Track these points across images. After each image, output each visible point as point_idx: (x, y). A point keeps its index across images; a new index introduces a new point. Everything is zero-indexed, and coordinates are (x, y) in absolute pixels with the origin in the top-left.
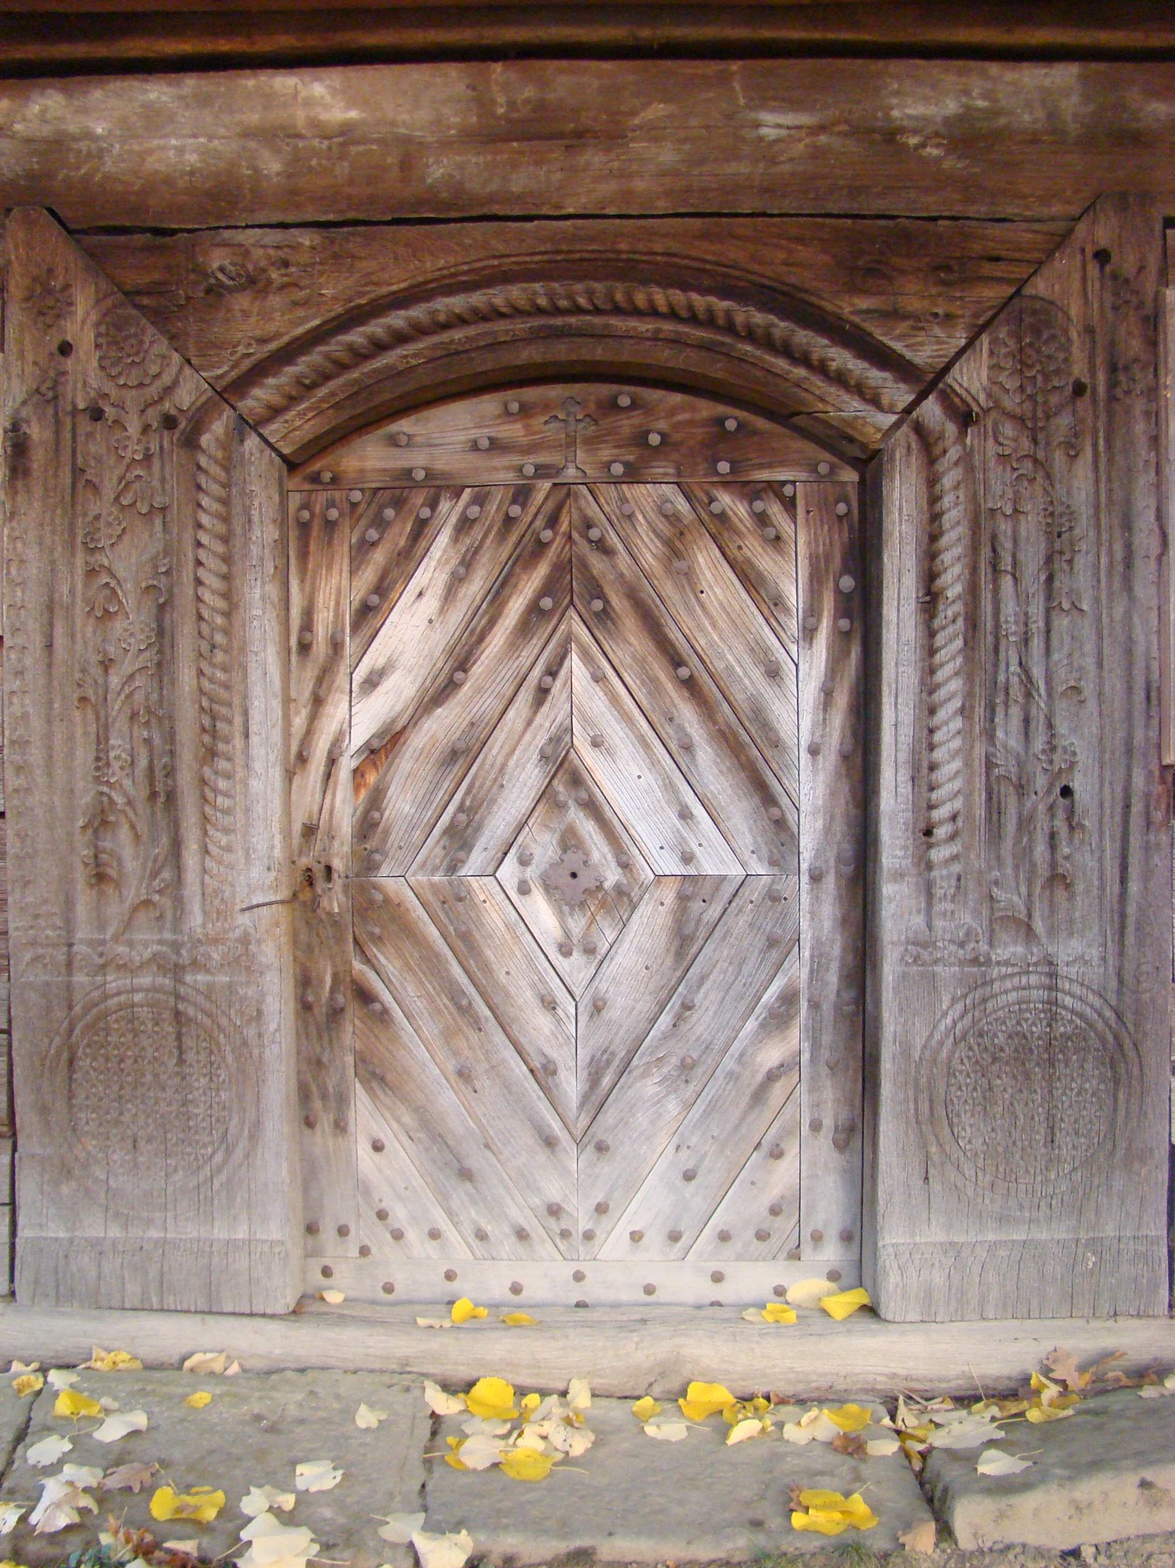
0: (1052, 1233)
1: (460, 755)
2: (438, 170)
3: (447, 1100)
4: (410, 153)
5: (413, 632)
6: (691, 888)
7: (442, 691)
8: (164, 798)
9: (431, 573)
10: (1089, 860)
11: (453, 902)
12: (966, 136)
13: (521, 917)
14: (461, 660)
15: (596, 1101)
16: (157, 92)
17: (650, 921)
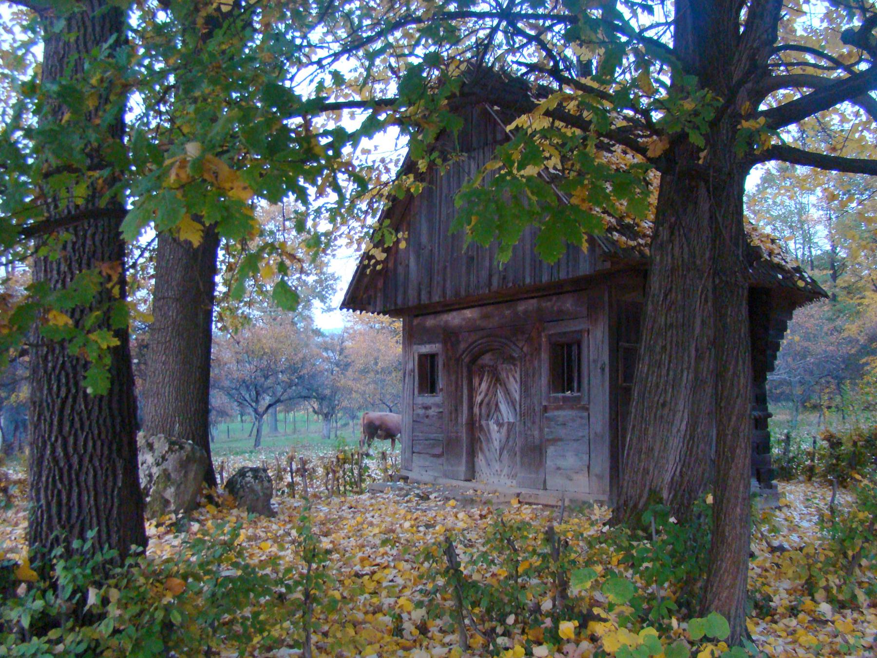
0: (533, 476)
1: (488, 404)
2: (478, 322)
3: (487, 454)
4: (475, 320)
5: (484, 386)
6: (509, 423)
7: (486, 395)
8: (456, 410)
9: (485, 378)
10: (537, 420)
11: (488, 425)
12: (525, 312)
13: (494, 427)
14: (488, 390)
15: (501, 454)
16: (455, 313)
17: (505, 428)
